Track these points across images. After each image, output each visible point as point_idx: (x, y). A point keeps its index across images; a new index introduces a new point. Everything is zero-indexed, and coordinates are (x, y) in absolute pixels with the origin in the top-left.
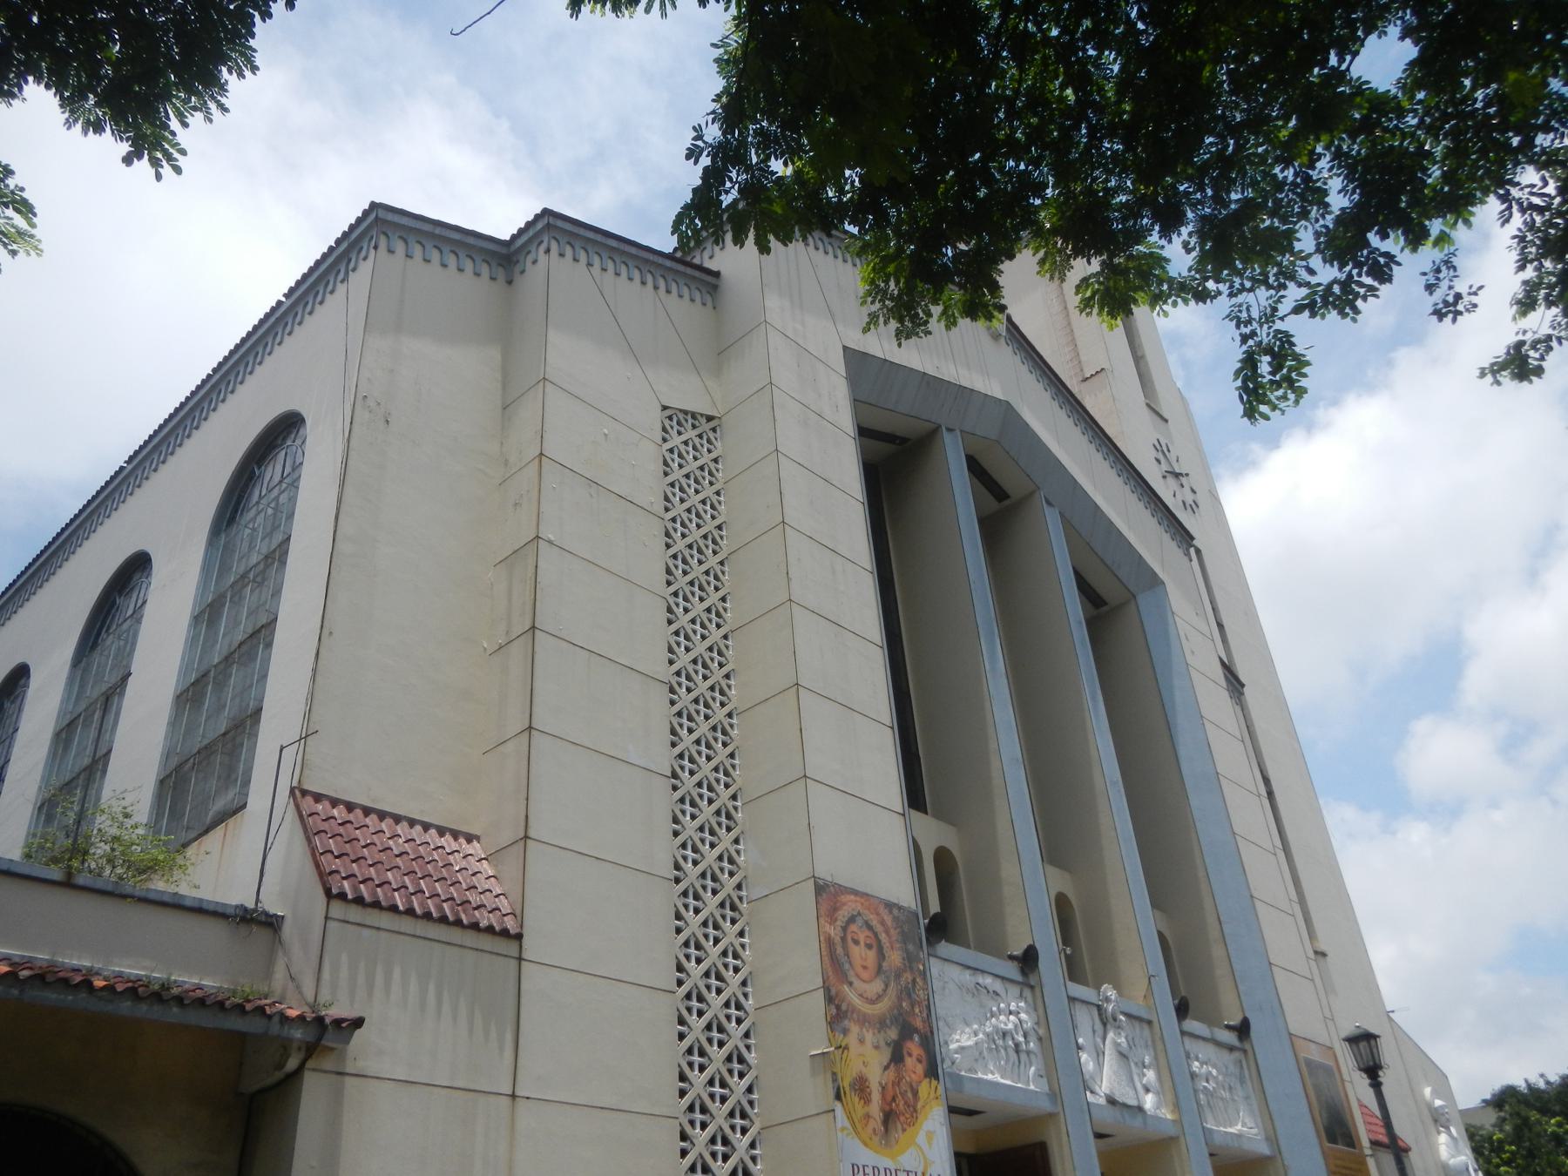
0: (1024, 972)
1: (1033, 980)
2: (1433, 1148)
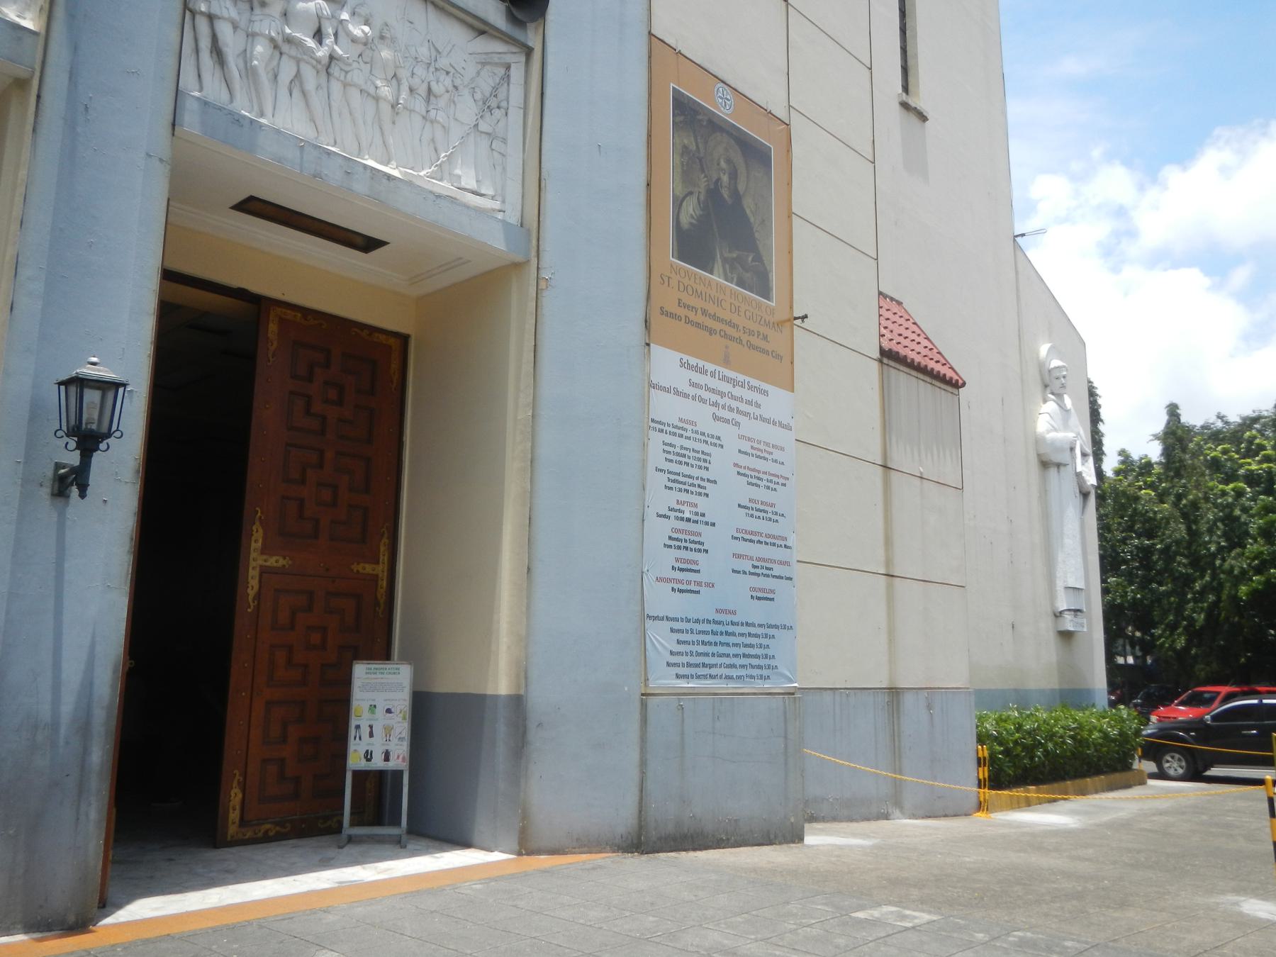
2: (1028, 418)
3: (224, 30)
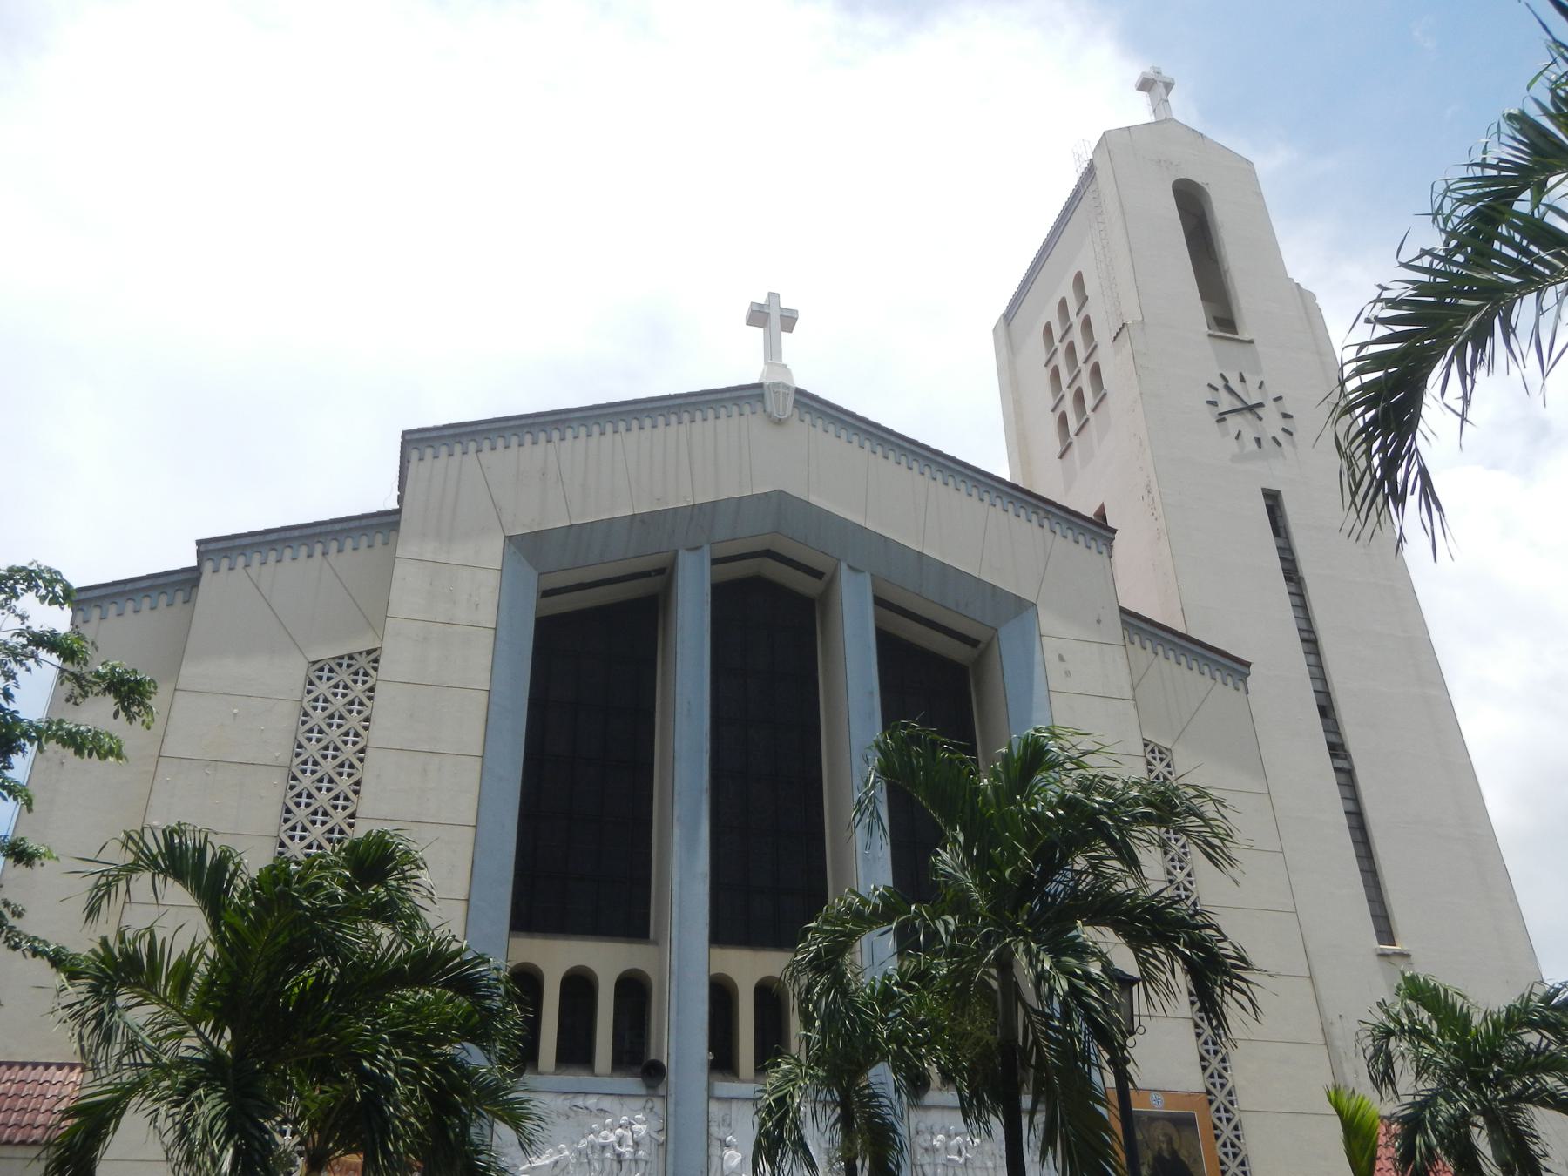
0: (649, 1087)
1: (661, 1091)
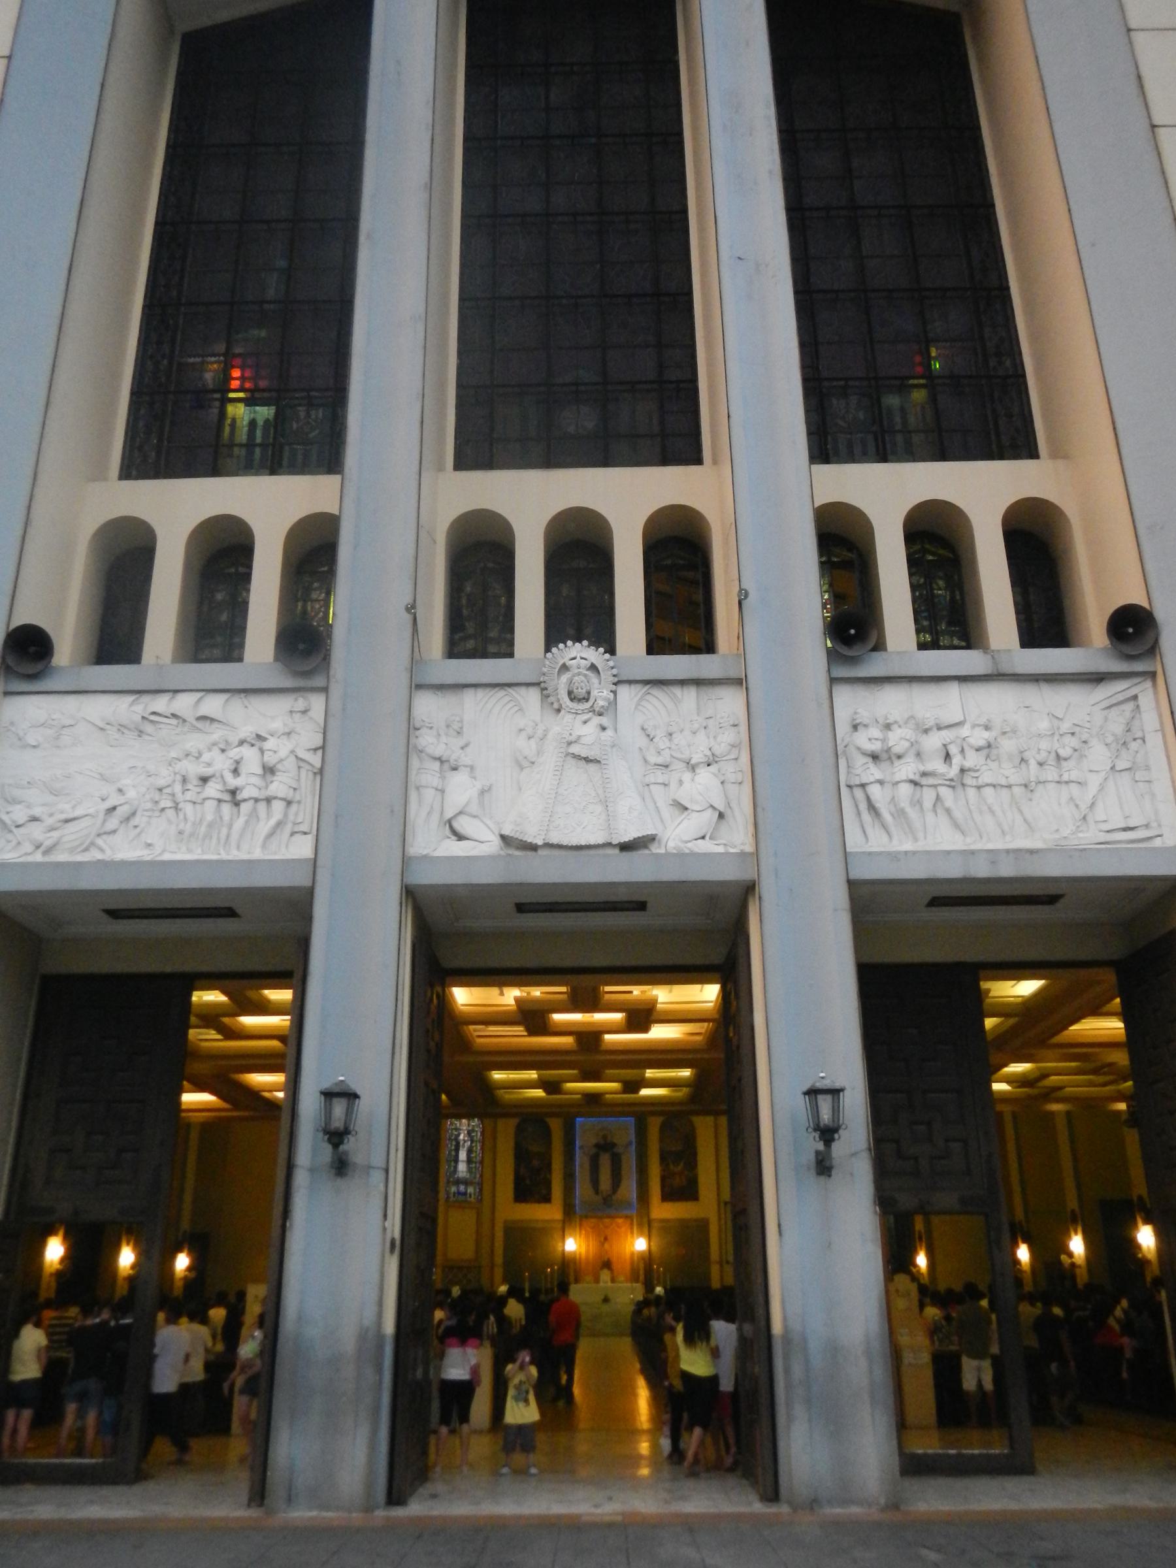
3: (875, 791)
